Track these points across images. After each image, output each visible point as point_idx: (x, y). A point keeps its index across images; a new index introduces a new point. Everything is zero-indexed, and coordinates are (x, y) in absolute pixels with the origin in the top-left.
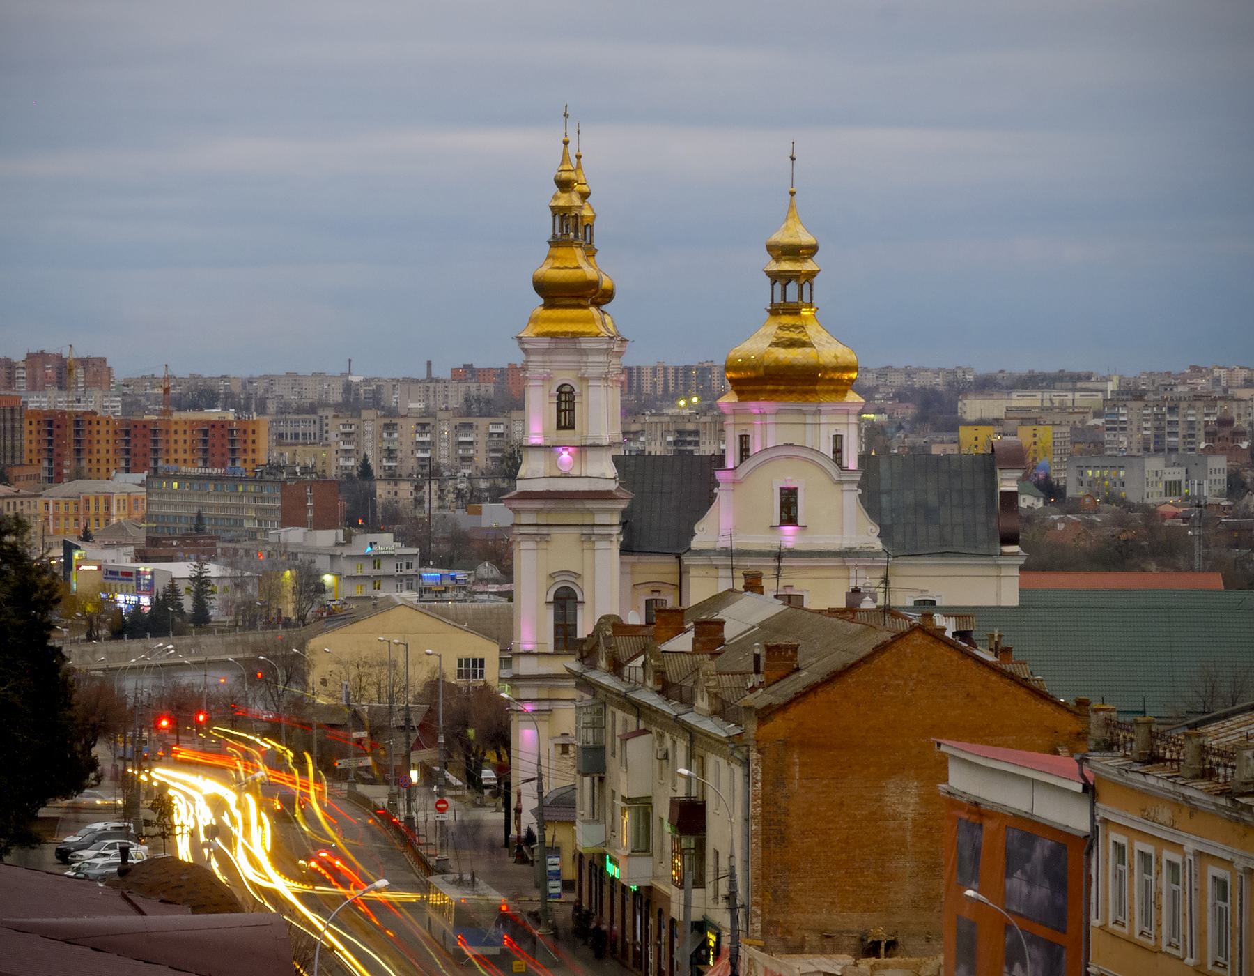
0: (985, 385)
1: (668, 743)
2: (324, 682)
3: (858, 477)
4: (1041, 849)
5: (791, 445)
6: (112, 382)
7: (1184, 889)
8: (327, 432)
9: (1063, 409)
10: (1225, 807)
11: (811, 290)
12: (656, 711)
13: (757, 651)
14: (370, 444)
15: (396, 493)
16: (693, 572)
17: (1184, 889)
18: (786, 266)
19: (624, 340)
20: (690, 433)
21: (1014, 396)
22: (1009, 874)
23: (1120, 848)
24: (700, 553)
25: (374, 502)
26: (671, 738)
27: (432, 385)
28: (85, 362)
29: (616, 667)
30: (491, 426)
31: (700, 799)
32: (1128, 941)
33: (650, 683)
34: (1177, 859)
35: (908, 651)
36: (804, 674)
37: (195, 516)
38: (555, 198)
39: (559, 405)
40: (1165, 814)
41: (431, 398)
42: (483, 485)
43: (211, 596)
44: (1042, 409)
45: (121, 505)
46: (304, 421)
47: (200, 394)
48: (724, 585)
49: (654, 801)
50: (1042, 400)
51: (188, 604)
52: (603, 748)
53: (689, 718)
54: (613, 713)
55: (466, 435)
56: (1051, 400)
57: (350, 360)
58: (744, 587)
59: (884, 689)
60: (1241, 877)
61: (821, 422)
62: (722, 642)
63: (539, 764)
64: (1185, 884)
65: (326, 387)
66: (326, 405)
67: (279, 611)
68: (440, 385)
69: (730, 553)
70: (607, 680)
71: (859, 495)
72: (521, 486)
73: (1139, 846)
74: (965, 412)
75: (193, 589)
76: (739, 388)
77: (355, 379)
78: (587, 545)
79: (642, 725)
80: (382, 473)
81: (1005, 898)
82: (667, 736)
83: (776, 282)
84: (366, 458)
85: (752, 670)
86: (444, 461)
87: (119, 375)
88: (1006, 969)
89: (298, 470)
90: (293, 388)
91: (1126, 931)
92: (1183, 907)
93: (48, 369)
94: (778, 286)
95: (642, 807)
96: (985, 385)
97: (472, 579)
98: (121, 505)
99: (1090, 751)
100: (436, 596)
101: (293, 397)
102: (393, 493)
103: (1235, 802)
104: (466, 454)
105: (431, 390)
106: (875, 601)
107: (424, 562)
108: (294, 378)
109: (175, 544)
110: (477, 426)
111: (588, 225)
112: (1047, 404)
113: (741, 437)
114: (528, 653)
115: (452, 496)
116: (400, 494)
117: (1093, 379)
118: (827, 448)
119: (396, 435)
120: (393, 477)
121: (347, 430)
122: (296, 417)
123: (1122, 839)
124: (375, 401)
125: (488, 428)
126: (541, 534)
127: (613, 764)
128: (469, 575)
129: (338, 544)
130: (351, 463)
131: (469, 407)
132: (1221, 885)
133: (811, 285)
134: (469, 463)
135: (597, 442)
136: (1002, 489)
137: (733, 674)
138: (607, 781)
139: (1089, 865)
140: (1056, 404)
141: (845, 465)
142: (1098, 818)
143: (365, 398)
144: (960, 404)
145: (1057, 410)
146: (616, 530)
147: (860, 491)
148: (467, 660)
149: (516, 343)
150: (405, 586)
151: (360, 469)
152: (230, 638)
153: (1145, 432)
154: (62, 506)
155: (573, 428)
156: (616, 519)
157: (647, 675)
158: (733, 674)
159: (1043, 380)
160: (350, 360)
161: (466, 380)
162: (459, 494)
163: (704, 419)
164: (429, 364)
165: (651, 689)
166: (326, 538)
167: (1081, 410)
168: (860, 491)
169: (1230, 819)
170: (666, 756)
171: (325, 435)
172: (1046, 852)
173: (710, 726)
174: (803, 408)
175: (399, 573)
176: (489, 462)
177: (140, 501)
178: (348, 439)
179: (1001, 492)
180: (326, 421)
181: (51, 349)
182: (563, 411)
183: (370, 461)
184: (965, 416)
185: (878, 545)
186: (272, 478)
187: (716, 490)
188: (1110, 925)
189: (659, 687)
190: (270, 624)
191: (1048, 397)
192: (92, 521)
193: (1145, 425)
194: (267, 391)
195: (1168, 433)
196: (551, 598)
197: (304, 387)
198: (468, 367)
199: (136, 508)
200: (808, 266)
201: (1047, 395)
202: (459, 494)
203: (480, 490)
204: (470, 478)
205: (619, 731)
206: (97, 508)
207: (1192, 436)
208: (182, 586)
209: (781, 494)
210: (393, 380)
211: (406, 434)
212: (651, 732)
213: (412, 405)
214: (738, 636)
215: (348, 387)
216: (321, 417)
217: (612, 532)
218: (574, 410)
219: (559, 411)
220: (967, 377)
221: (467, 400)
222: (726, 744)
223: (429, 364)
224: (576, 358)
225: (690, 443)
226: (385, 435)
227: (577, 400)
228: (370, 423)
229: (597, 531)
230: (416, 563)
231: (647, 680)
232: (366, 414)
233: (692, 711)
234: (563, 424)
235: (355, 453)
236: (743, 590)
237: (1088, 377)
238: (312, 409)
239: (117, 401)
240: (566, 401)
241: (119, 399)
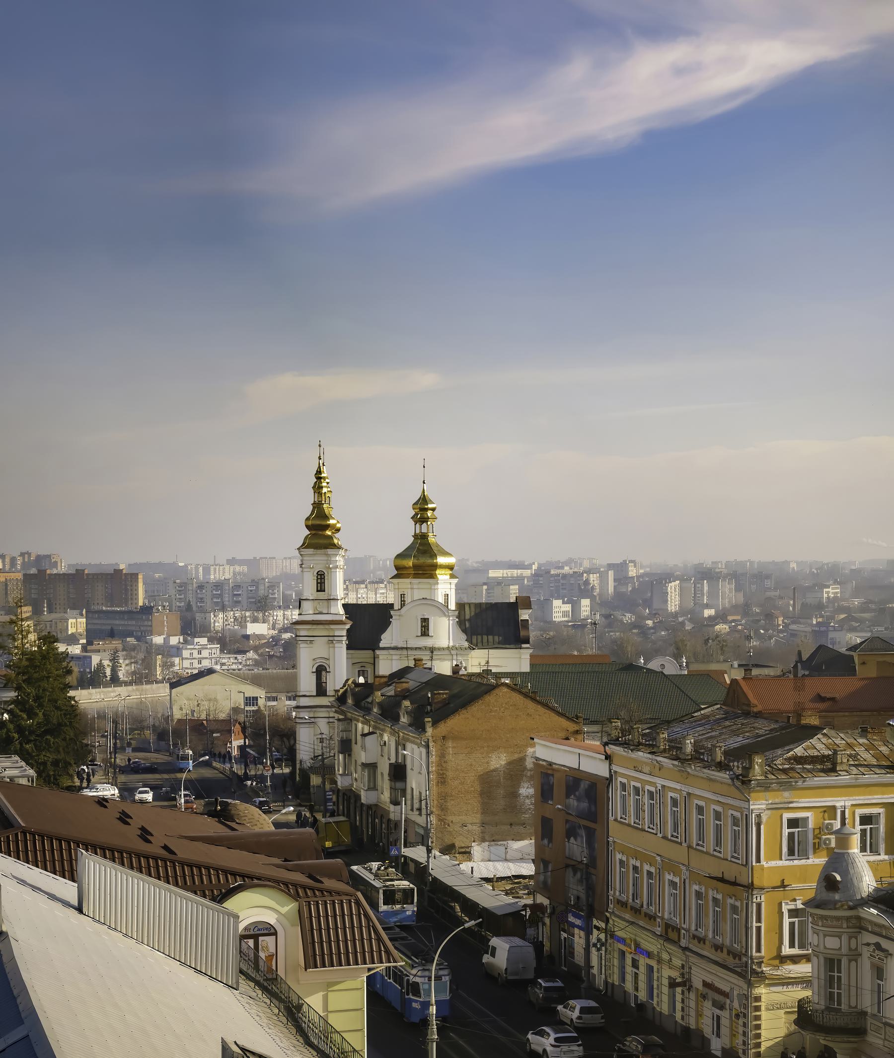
2: (181, 709)
4: (583, 785)
5: (426, 598)
7: (656, 803)
10: (678, 766)
16: (381, 657)
17: (656, 803)
22: (568, 796)
23: (623, 786)
24: (384, 649)
25: (195, 623)
27: (217, 567)
31: (403, 763)
32: (629, 825)
34: (653, 789)
36: (452, 705)
39: (317, 580)
40: (646, 769)
49: (379, 765)
51: (108, 672)
60: (685, 797)
64: (657, 800)
69: (407, 648)
73: (633, 783)
75: (111, 665)
78: (331, 645)
81: (567, 806)
88: (566, 840)
91: (627, 822)
92: (657, 811)
95: (372, 767)
97: (244, 659)
102: (204, 618)
103: (682, 763)
105: (217, 569)
106: (466, 670)
119: (204, 591)
123: (624, 781)
125: (247, 587)
126: (310, 640)
127: (356, 748)
130: (182, 604)
132: (675, 802)
138: (353, 756)
139: (608, 792)
141: (449, 608)
142: (612, 771)
146: (345, 638)
147: (457, 620)
148: (250, 697)
152: (130, 688)
153: (551, 588)
155: (324, 591)
156: (344, 633)
169: (679, 771)
172: (586, 786)
179: (521, 620)
183: (191, 603)
187: (391, 620)
188: (619, 819)
193: (551, 585)
195: (562, 588)
201: (505, 571)
207: (572, 590)
208: (106, 663)
219: (317, 583)
224: (326, 558)
226: (198, 591)
227: (326, 578)
229: (336, 638)
234: (319, 589)
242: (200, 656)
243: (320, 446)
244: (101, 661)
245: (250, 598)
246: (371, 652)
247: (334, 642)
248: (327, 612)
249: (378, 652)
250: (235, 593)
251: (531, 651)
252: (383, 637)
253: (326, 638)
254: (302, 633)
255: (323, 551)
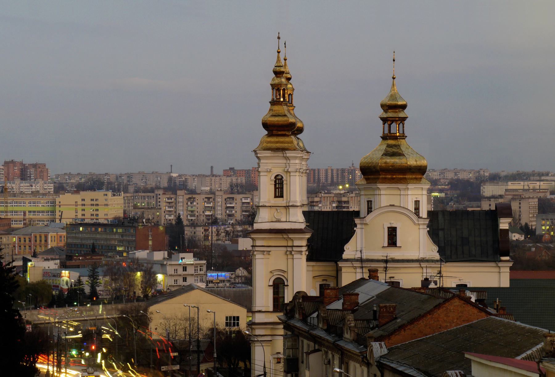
0: (494, 178)
1: (330, 356)
3: (427, 222)
5: (393, 205)
6: (49, 176)
8: (160, 202)
9: (534, 190)
11: (403, 127)
12: (324, 339)
13: (375, 309)
14: (182, 208)
15: (195, 233)
16: (344, 270)
18: (390, 114)
19: (308, 152)
20: (345, 202)
21: (510, 183)
24: (347, 260)
25: (183, 238)
26: (332, 353)
27: (213, 178)
28: (35, 166)
29: (304, 319)
30: (243, 199)
33: (321, 325)
35: (452, 308)
36: (399, 320)
37: (91, 245)
38: (273, 79)
39: (275, 185)
41: (213, 185)
42: (239, 228)
43: (100, 285)
44: (524, 190)
45: (53, 239)
46: (148, 197)
47: (94, 183)
48: (359, 276)
50: (524, 186)
52: (297, 359)
53: (341, 343)
54: (302, 342)
55: (231, 204)
56: (528, 185)
57: (171, 166)
58: (369, 277)
59: (440, 328)
61: (409, 194)
62: (357, 304)
63: (265, 367)
65: (159, 179)
66: (158, 188)
67: (135, 293)
68: (218, 178)
69: (361, 260)
70: (299, 324)
71: (428, 231)
72: (256, 226)
74: (484, 192)
76: (366, 177)
77: (174, 175)
79: (317, 347)
80: (188, 223)
82: (330, 352)
83: (385, 123)
84: (179, 216)
85: (372, 318)
86: (219, 217)
87: (52, 173)
89: (144, 220)
90: (142, 180)
93: (15, 169)
94: (386, 125)
96: (494, 178)
97: (233, 276)
98: (53, 239)
99: (543, 357)
100: (215, 285)
101: (142, 184)
104: (230, 213)
105: (213, 181)
106: (436, 284)
107: (209, 268)
108: (144, 175)
109: (81, 259)
110: (236, 200)
111: (290, 94)
112: (526, 187)
113: (368, 201)
114: (260, 312)
115: (223, 234)
116: (197, 233)
117: (550, 175)
118: (412, 207)
119: (195, 203)
120: (193, 225)
121: (170, 201)
122: (143, 194)
124: (184, 186)
125: (241, 199)
128: (232, 274)
129: (164, 259)
131: (232, 189)
133: (403, 124)
134: (232, 218)
135: (295, 204)
136: (501, 228)
137: (363, 320)
140: (531, 188)
141: (421, 216)
143: (179, 185)
144: (482, 188)
145: (532, 191)
146: (304, 249)
147: (428, 229)
148: (230, 317)
149: (253, 153)
150: (199, 280)
151: (176, 221)
154: (22, 240)
156: (304, 243)
157: (319, 322)
158: (363, 320)
159: (524, 176)
160: (171, 166)
161: (230, 176)
162: (227, 233)
163: (351, 195)
164: (212, 167)
165: (321, 328)
166: (159, 256)
167: (544, 191)
168: (428, 229)
170: (329, 362)
171: (159, 204)
173: (351, 347)
174: (399, 187)
175: (196, 273)
176: (242, 217)
177: (63, 237)
178: (170, 205)
179: (501, 230)
180: (159, 196)
181: (18, 159)
182: (277, 188)
183: (181, 217)
184: (484, 194)
185: (437, 256)
186: (131, 225)
187: (355, 229)
189: (325, 327)
190: (129, 300)
191: (527, 184)
192: (38, 246)
194: (129, 181)
196: (271, 283)
197: (148, 179)
198: (232, 169)
199: (61, 241)
200: (401, 115)
201: (526, 183)
202: (227, 233)
203: (238, 231)
204: (233, 225)
205: (305, 350)
206: (41, 241)
208: (85, 279)
209: (388, 230)
210: (193, 175)
211: (200, 204)
212: (321, 351)
213: (203, 188)
214: (366, 301)
215: (170, 179)
216: (157, 194)
217: (302, 250)
218: (283, 188)
219: (275, 188)
220: (486, 174)
221: (231, 186)
222: (359, 356)
223: (212, 167)
224: (285, 161)
225: (344, 207)
227: (285, 182)
228: (182, 197)
229: (295, 249)
230: (204, 268)
231: (320, 324)
232: (179, 192)
233: (342, 340)
234: (277, 195)
235: (174, 212)
236: (368, 278)
237: (547, 174)
238: (152, 190)
239: (51, 186)
240: (279, 184)
241: (52, 185)
242: (185, 273)
243: (279, 38)
244: (79, 277)
245: (243, 211)
246: (333, 264)
247: (293, 253)
248: (285, 220)
249: (341, 264)
250: (228, 205)
251: (511, 264)
252: (346, 247)
253: (284, 249)
254: (258, 243)
255: (280, 154)
